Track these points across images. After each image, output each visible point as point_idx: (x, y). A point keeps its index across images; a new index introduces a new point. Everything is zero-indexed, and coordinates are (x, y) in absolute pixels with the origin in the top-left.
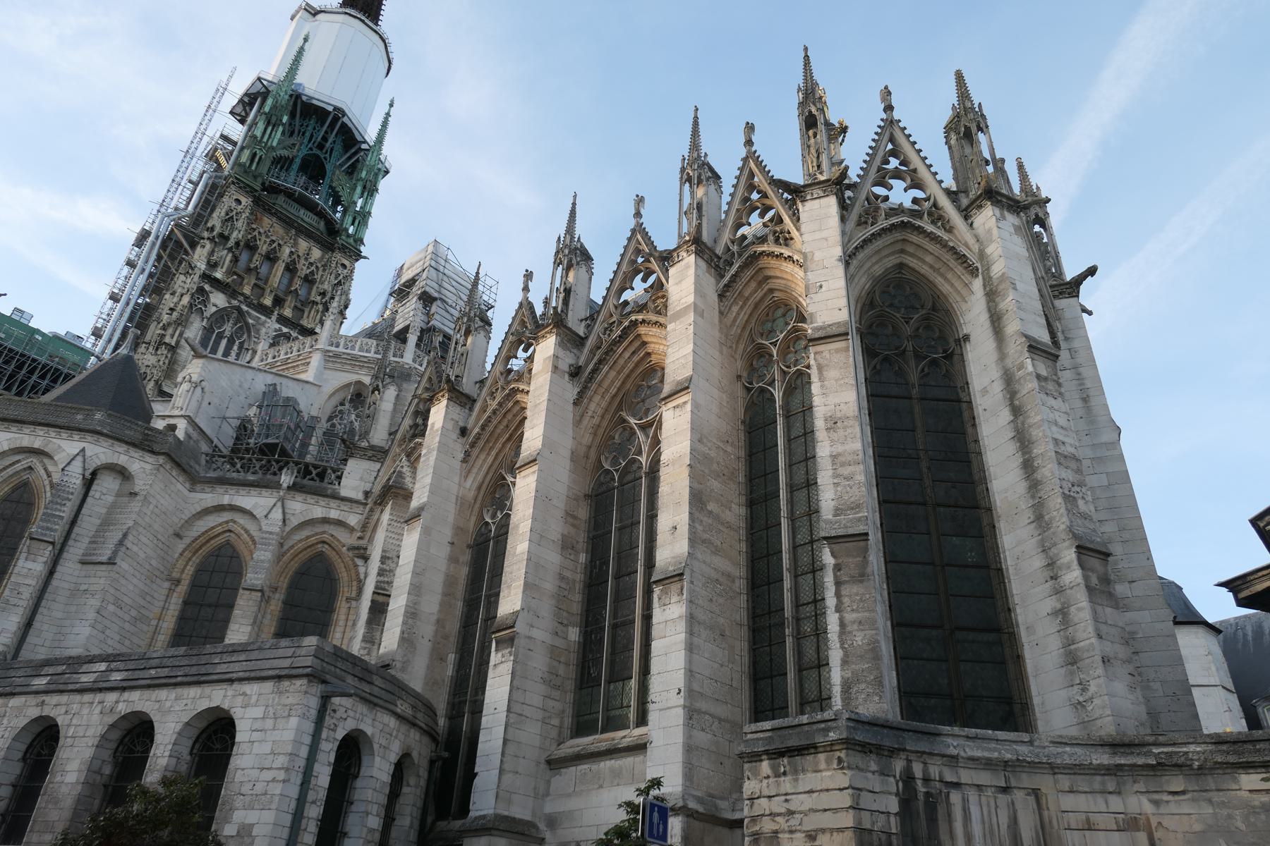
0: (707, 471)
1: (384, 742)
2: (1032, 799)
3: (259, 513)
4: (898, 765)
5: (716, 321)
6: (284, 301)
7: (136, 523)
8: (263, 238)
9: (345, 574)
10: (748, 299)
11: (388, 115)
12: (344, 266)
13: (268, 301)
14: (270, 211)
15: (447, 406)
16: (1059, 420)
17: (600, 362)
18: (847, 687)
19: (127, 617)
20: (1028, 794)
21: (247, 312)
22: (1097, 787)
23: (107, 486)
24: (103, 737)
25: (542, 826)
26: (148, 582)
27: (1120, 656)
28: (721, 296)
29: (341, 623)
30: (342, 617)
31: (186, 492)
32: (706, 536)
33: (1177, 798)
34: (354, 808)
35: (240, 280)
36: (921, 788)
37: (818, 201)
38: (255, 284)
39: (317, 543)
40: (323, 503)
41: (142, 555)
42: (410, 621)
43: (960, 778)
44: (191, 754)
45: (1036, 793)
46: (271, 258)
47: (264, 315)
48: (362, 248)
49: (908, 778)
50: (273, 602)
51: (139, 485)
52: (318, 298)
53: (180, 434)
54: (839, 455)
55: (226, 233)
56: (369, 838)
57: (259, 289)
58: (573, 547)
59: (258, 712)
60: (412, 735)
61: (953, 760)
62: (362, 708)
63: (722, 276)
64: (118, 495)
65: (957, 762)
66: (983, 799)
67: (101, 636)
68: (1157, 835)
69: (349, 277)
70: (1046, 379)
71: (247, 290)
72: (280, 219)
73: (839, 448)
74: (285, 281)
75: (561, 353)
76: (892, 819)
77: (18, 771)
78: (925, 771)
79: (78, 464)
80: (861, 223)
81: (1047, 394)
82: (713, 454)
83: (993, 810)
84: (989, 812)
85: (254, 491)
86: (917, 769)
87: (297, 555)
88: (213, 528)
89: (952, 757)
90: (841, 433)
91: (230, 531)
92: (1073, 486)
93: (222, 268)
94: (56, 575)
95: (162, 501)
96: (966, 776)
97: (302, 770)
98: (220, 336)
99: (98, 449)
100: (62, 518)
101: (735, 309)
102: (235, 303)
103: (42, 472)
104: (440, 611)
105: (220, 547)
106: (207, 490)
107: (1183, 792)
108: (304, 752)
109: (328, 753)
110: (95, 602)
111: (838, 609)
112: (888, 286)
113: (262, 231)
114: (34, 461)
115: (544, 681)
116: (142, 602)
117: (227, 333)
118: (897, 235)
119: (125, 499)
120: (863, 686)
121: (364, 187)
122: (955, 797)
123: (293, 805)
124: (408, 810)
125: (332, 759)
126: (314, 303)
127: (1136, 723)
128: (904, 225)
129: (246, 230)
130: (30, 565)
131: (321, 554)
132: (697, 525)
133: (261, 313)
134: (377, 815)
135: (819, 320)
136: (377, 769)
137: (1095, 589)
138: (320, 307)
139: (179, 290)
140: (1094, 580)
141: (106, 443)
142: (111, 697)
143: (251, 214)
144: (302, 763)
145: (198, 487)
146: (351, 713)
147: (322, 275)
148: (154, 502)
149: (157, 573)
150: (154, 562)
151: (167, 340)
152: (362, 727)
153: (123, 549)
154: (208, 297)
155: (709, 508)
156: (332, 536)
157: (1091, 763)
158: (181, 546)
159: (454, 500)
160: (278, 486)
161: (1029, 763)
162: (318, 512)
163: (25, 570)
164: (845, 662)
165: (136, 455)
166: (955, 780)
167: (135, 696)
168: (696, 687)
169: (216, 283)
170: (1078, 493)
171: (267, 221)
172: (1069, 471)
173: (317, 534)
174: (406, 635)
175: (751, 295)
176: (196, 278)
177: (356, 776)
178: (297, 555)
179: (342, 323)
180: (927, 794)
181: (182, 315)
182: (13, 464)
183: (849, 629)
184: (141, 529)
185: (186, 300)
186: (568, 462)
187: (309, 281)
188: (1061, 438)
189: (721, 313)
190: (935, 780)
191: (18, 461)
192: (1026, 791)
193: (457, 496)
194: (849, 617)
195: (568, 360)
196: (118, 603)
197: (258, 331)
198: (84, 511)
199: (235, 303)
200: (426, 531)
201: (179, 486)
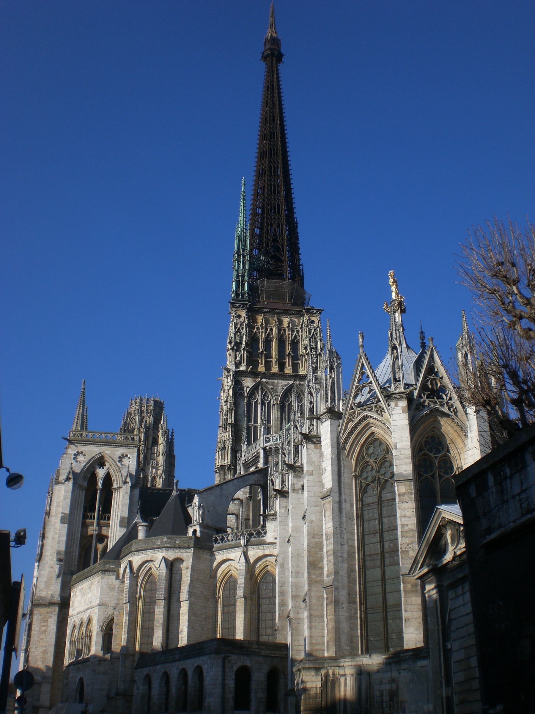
0: (317, 550)
21: (267, 382)
27: (415, 617)
37: (325, 422)
47: (276, 379)
49: (327, 675)
53: (198, 534)
54: (328, 551)
75: (295, 481)
86: (331, 672)
88: (224, 570)
92: (408, 545)
93: (244, 363)
94: (172, 609)
98: (256, 404)
102: (258, 380)
103: (155, 569)
108: (220, 678)
111: (327, 616)
114: (151, 564)
117: (259, 401)
120: (331, 643)
122: (342, 680)
125: (234, 677)
130: (159, 610)
133: (274, 379)
135: (325, 487)
137: (409, 591)
139: (226, 388)
140: (409, 586)
142: (177, 663)
147: (302, 335)
150: (205, 593)
163: (158, 612)
164: (327, 634)
167: (182, 663)
168: (314, 641)
172: (407, 539)
181: (231, 403)
185: (231, 392)
188: (406, 523)
191: (146, 566)
198: (173, 580)
199: (258, 380)
201: (205, 556)
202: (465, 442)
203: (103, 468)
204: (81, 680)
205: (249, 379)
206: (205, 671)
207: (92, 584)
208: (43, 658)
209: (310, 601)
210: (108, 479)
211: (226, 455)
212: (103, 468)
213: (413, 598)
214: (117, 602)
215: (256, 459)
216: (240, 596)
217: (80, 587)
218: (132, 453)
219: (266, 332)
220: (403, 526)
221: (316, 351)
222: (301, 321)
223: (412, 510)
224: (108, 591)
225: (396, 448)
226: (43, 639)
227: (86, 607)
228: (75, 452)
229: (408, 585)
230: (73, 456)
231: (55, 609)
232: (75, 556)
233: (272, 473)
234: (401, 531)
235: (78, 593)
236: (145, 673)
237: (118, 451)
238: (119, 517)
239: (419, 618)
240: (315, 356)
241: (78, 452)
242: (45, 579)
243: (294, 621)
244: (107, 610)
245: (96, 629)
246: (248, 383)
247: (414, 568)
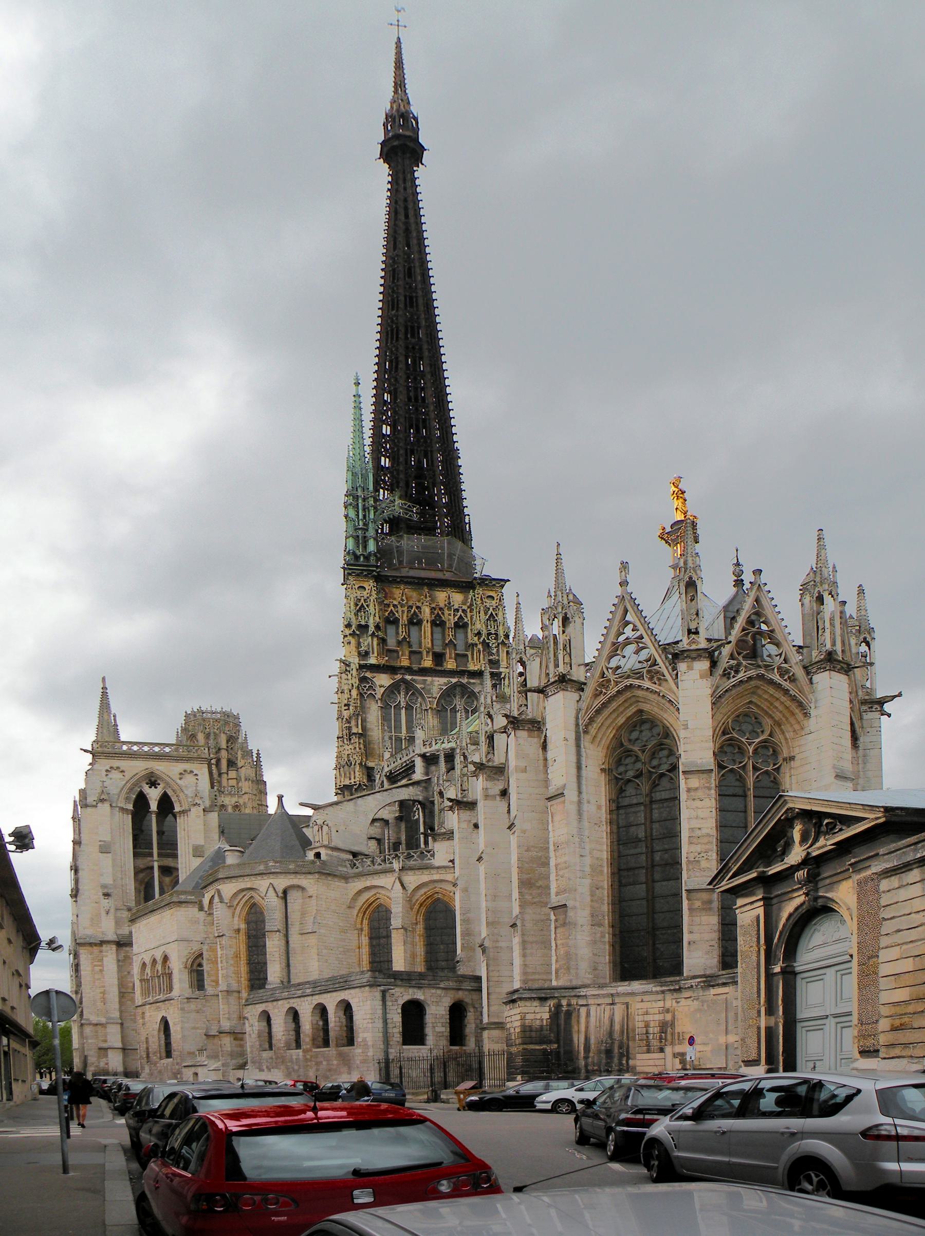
35: (395, 654)
38: (411, 652)
71: (405, 663)
74: (438, 636)
187: (461, 625)
211: (352, 773)
222: (470, 597)
227: (158, 943)
240: (494, 646)
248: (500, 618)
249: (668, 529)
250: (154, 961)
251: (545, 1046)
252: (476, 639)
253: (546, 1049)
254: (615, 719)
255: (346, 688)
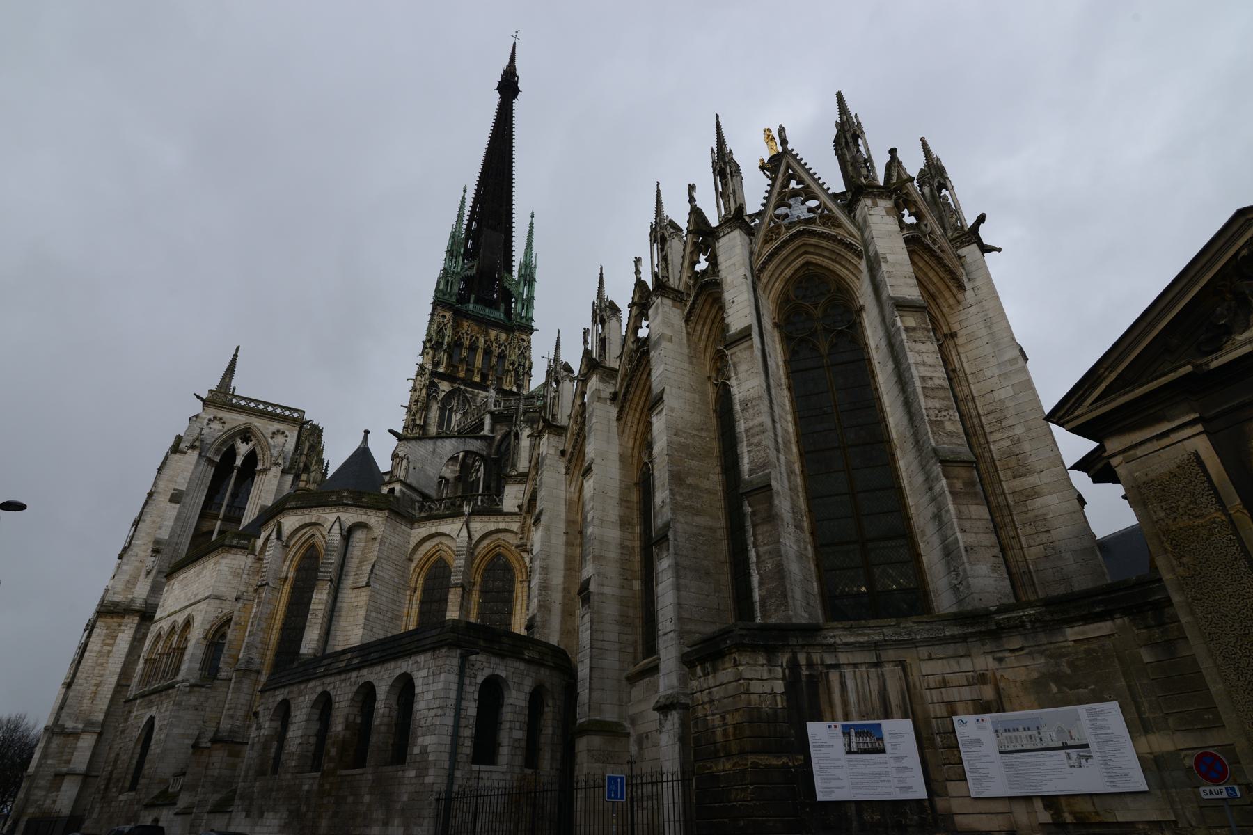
0: (683, 456)
1: (516, 680)
2: (899, 669)
3: (454, 534)
4: (784, 658)
5: (685, 341)
6: (488, 375)
7: (378, 557)
8: (465, 336)
9: (517, 565)
10: (706, 318)
11: (531, 224)
12: (523, 340)
13: (477, 379)
14: (467, 316)
15: (548, 438)
16: (926, 359)
17: (628, 386)
18: (763, 601)
19: (386, 619)
20: (897, 665)
21: (465, 390)
22: (950, 652)
23: (359, 536)
24: (352, 699)
25: (627, 724)
26: (395, 593)
28: (687, 321)
29: (520, 599)
30: (520, 594)
31: (408, 530)
32: (687, 503)
33: (1017, 654)
34: (503, 727)
36: (805, 672)
39: (496, 547)
40: (494, 520)
41: (387, 577)
42: (543, 593)
43: (838, 660)
44: (398, 704)
45: (902, 664)
46: (473, 348)
48: (533, 324)
49: (794, 665)
50: (474, 592)
51: (378, 532)
52: (511, 367)
53: (397, 493)
54: (751, 428)
55: (440, 340)
56: (517, 744)
57: (470, 371)
58: (629, 523)
59: (424, 673)
60: (542, 672)
61: (832, 648)
62: (495, 660)
63: (686, 305)
64: (366, 542)
65: (835, 649)
66: (858, 674)
67: (371, 634)
68: (1002, 685)
69: (528, 347)
70: (914, 329)
71: (462, 374)
72: (473, 320)
73: (751, 424)
75: (601, 386)
76: (779, 698)
77: (318, 727)
78: (809, 659)
79: (337, 526)
80: (766, 241)
81: (915, 341)
82: (689, 441)
83: (866, 681)
84: (863, 683)
85: (449, 520)
86: (802, 659)
87: (484, 558)
88: (430, 550)
89: (830, 645)
90: (751, 411)
91: (440, 550)
92: (940, 411)
95: (393, 539)
96: (843, 658)
97: (453, 706)
99: (348, 515)
100: (332, 563)
101: (699, 328)
102: (456, 385)
104: (564, 582)
105: (436, 562)
106: (422, 526)
107: (1022, 649)
108: (453, 695)
109: (472, 692)
110: (362, 613)
112: (801, 282)
113: (464, 332)
114: (314, 530)
115: (617, 622)
116: (395, 607)
118: (798, 242)
119: (370, 543)
120: (773, 600)
121: (525, 280)
122: (834, 676)
123: (450, 730)
124: (549, 723)
125: (476, 696)
126: (509, 371)
127: (999, 596)
128: (800, 233)
129: (453, 334)
130: (319, 596)
131: (499, 554)
132: (678, 498)
134: (521, 729)
136: (516, 700)
137: (960, 493)
138: (513, 373)
140: (959, 485)
141: (351, 509)
142: (354, 675)
143: (454, 322)
144: (453, 702)
145: (416, 524)
146: (487, 665)
148: (388, 541)
149: (401, 586)
150: (396, 580)
151: (418, 422)
152: (497, 672)
153: (373, 575)
154: (438, 387)
155: (688, 482)
156: (504, 540)
157: (944, 635)
158: (413, 566)
159: (564, 503)
160: (463, 515)
161: (893, 641)
162: (491, 526)
164: (761, 584)
165: (371, 514)
166: (834, 662)
167: (365, 672)
168: (685, 615)
169: (443, 377)
170: (945, 416)
171: (466, 324)
172: (936, 400)
173: (493, 541)
174: (542, 603)
175: (708, 315)
176: (427, 376)
177: (502, 705)
178: (484, 558)
179: (530, 380)
180: (809, 676)
181: (423, 403)
182: (303, 535)
183: (763, 558)
184: (382, 561)
185: (424, 392)
186: (618, 463)
187: (502, 357)
188: (928, 374)
189: (688, 333)
190: (817, 664)
192: (894, 663)
193: (566, 500)
194: (762, 550)
195: (608, 390)
196: (377, 610)
197: (475, 401)
198: (348, 556)
199: (456, 385)
200: (547, 529)
201: (403, 527)
202: (960, 297)
203: (247, 443)
204: (152, 719)
205: (446, 383)
206: (418, 683)
207: (203, 569)
208: (95, 693)
209: (675, 540)
210: (251, 458)
212: (247, 443)
213: (973, 508)
214: (244, 589)
215: (481, 425)
216: (456, 584)
217: (182, 577)
218: (292, 431)
219: (471, 340)
220: (923, 379)
221: (523, 369)
223: (935, 355)
224: (229, 577)
225: (886, 262)
226: (102, 664)
228: (211, 417)
229: (956, 481)
230: (206, 421)
231: (133, 620)
232: (183, 550)
233: (518, 423)
234: (923, 388)
235: (176, 585)
236: (280, 698)
237: (271, 425)
238: (259, 506)
239: (994, 547)
241: (215, 418)
242: (127, 577)
243: (596, 597)
244: (223, 606)
245: (196, 633)
246: (445, 387)
247: (1073, 400)
248: (527, 355)
249: (766, 161)
250: (173, 629)
251: (785, 760)
252: (511, 367)
253: (785, 766)
254: (783, 271)
255: (418, 387)
